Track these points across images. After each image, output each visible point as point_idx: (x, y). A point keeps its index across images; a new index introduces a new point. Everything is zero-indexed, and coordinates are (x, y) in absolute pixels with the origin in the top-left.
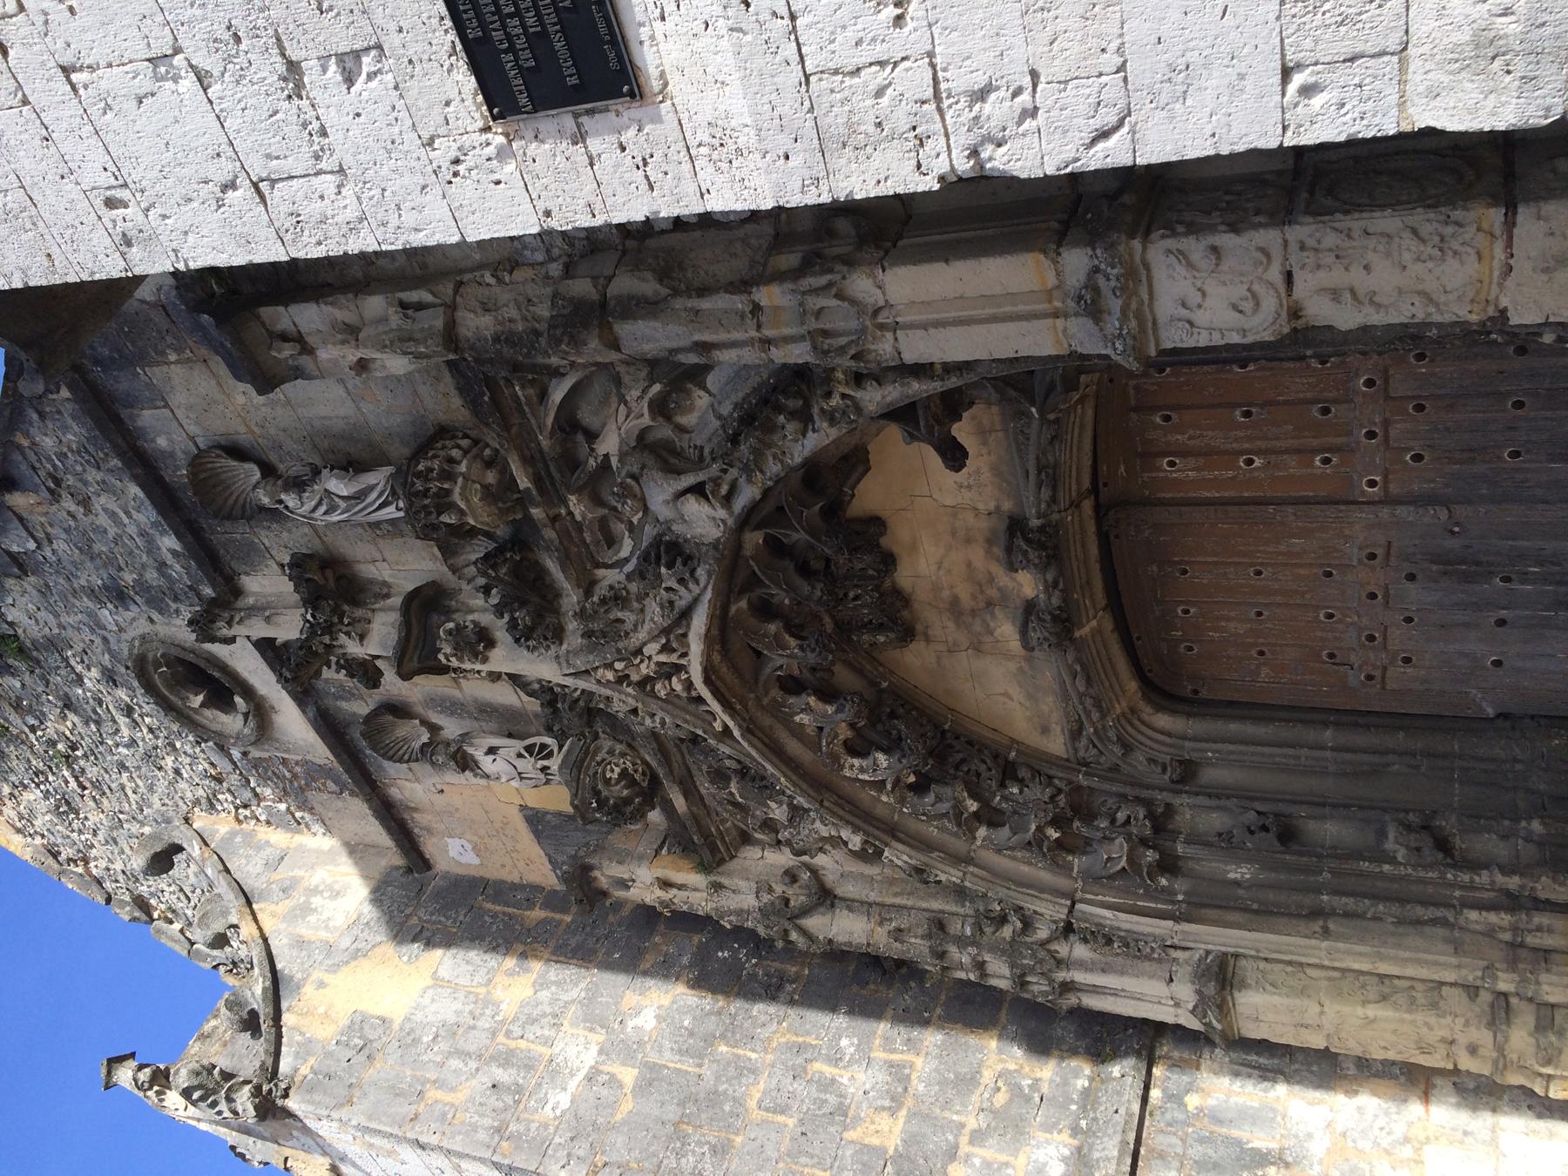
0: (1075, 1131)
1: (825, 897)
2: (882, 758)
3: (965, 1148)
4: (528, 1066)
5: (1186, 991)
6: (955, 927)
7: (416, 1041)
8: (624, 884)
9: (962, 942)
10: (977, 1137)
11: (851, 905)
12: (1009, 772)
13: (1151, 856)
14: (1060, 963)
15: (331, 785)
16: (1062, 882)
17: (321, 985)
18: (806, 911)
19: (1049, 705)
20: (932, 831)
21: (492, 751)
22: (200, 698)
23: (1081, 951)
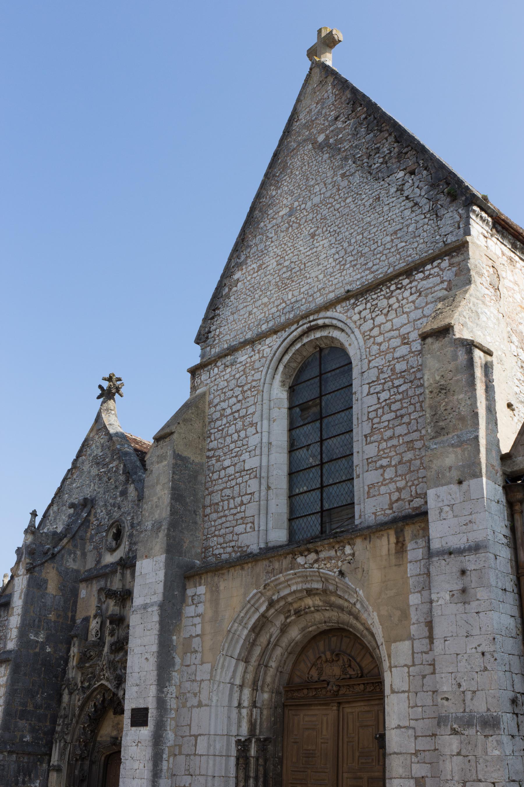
0: (32, 742)
1: (70, 694)
2: (93, 710)
3: (28, 722)
4: (39, 627)
5: (56, 763)
6: (66, 720)
7: (42, 598)
8: (74, 645)
9: (63, 722)
10: (30, 724)
11: (70, 698)
12: (92, 731)
13: (78, 757)
14: (60, 741)
15: (98, 559)
16: (74, 740)
17: (53, 568)
18: (68, 689)
19: (104, 739)
20: (82, 717)
21: (97, 623)
22: (115, 531)
23: (62, 744)
